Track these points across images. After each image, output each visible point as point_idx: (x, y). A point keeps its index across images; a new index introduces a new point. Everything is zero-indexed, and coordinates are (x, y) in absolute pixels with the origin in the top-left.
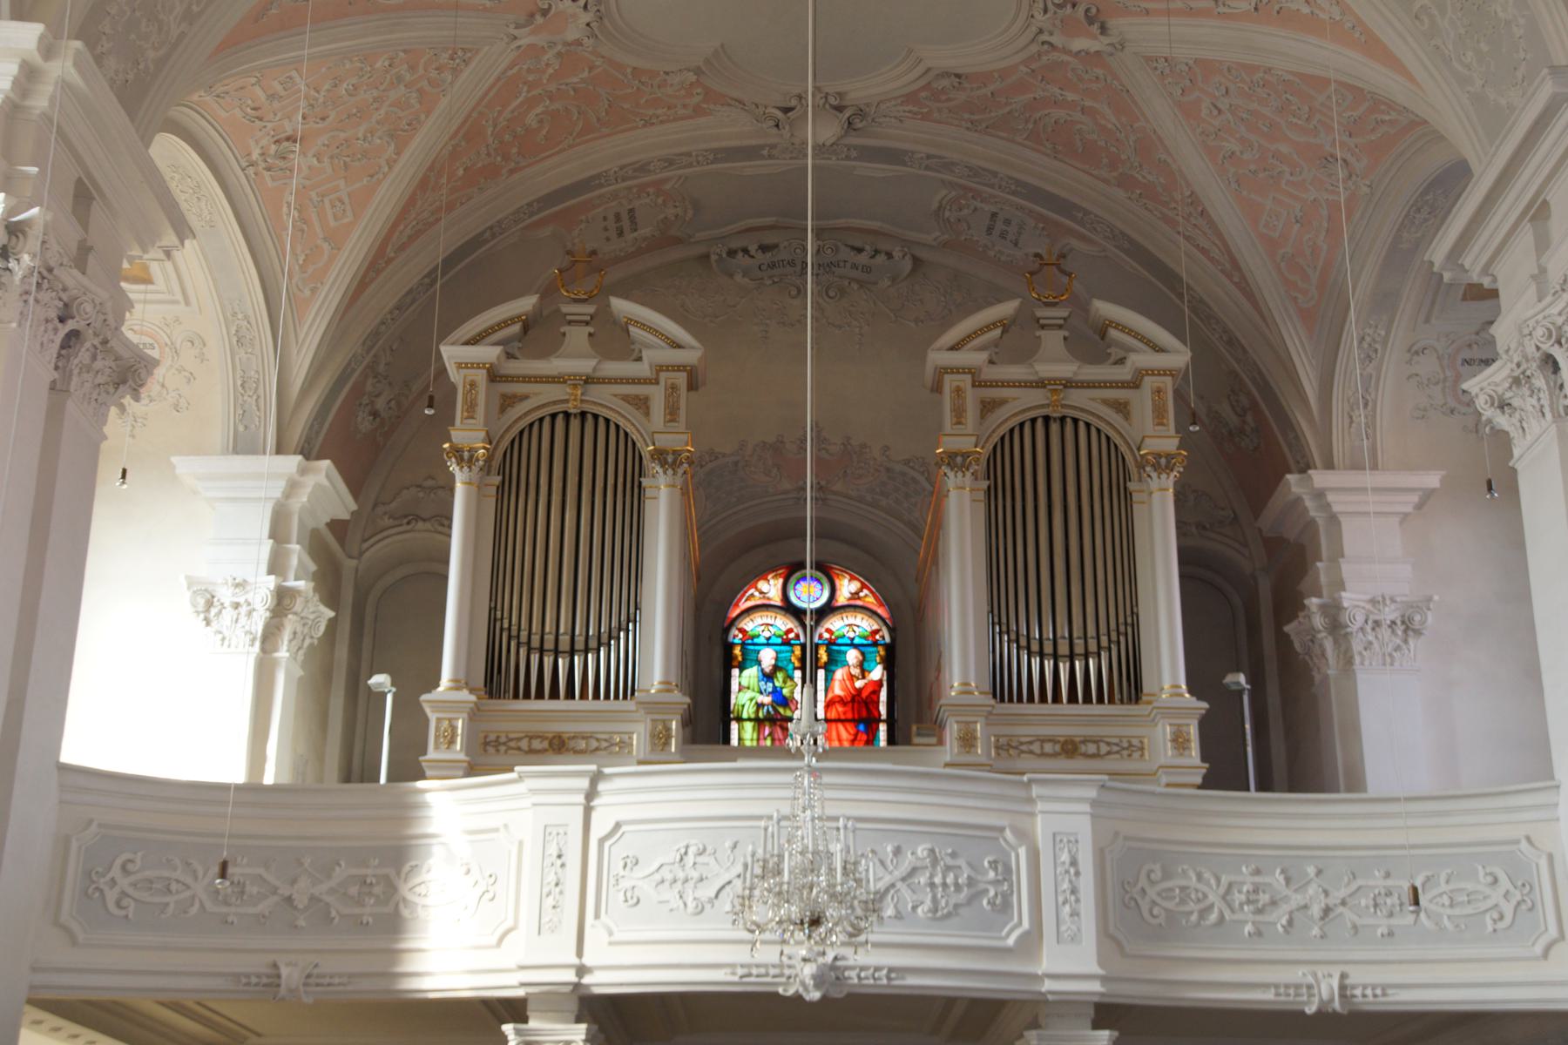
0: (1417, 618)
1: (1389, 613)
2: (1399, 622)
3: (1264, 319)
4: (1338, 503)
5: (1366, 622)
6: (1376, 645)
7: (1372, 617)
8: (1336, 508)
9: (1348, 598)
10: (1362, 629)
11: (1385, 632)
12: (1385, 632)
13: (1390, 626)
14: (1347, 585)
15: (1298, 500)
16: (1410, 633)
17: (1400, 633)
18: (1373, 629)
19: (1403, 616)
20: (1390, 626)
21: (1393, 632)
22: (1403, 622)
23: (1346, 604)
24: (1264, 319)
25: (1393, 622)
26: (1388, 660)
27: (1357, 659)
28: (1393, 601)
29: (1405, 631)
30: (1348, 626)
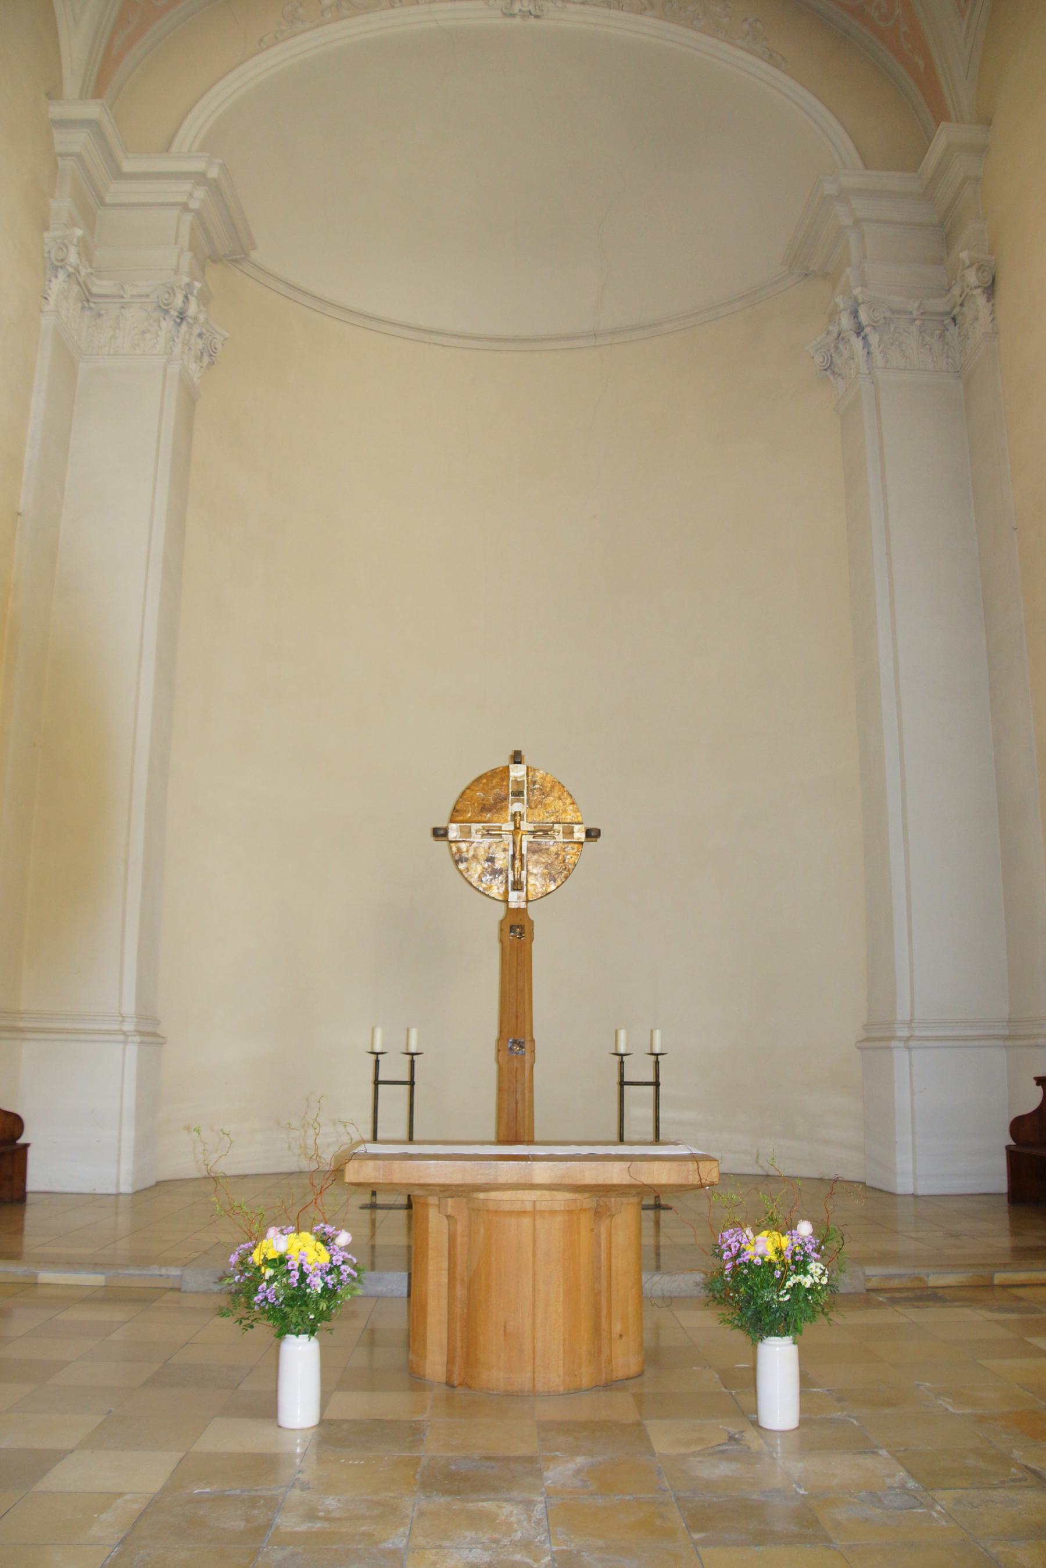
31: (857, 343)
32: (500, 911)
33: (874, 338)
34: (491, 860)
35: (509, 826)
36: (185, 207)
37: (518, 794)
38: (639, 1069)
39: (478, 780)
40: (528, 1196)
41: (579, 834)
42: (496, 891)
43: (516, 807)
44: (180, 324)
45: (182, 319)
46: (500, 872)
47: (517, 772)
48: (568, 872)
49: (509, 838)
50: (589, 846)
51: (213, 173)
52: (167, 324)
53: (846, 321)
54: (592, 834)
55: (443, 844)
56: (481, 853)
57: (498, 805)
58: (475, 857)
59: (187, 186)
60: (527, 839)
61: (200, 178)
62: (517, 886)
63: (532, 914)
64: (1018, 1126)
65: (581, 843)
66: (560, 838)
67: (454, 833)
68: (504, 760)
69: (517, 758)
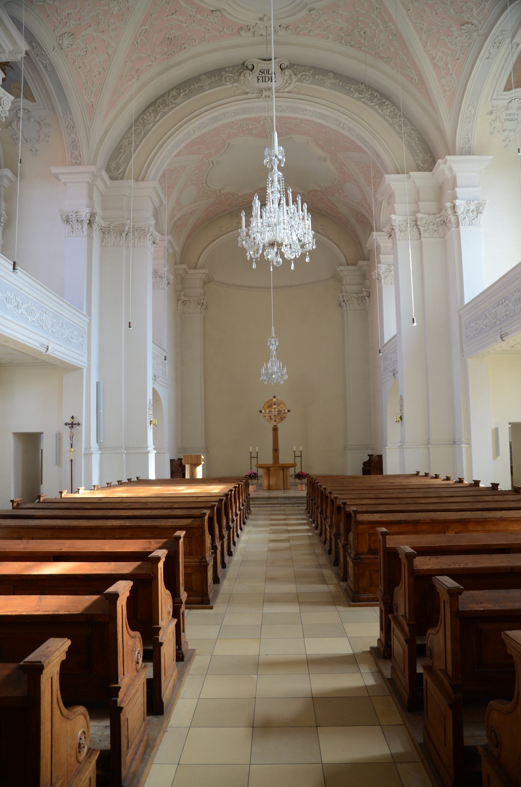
1: (472, 207)
2: (475, 210)
5: (464, 210)
6: (467, 219)
7: (466, 209)
8: (455, 169)
9: (458, 202)
10: (463, 213)
11: (470, 214)
12: (470, 214)
17: (475, 214)
18: (466, 213)
21: (473, 214)
23: (457, 204)
25: (473, 210)
26: (471, 223)
27: (460, 224)
29: (477, 213)
30: (457, 212)
31: (344, 304)
33: (347, 303)
36: (201, 278)
37: (275, 404)
38: (298, 454)
43: (275, 406)
44: (202, 306)
45: (203, 305)
47: (275, 400)
50: (288, 413)
51: (207, 272)
52: (199, 306)
53: (341, 299)
55: (261, 413)
57: (270, 406)
60: (277, 413)
61: (204, 273)
65: (286, 413)
67: (263, 411)
68: (272, 397)
69: (275, 397)
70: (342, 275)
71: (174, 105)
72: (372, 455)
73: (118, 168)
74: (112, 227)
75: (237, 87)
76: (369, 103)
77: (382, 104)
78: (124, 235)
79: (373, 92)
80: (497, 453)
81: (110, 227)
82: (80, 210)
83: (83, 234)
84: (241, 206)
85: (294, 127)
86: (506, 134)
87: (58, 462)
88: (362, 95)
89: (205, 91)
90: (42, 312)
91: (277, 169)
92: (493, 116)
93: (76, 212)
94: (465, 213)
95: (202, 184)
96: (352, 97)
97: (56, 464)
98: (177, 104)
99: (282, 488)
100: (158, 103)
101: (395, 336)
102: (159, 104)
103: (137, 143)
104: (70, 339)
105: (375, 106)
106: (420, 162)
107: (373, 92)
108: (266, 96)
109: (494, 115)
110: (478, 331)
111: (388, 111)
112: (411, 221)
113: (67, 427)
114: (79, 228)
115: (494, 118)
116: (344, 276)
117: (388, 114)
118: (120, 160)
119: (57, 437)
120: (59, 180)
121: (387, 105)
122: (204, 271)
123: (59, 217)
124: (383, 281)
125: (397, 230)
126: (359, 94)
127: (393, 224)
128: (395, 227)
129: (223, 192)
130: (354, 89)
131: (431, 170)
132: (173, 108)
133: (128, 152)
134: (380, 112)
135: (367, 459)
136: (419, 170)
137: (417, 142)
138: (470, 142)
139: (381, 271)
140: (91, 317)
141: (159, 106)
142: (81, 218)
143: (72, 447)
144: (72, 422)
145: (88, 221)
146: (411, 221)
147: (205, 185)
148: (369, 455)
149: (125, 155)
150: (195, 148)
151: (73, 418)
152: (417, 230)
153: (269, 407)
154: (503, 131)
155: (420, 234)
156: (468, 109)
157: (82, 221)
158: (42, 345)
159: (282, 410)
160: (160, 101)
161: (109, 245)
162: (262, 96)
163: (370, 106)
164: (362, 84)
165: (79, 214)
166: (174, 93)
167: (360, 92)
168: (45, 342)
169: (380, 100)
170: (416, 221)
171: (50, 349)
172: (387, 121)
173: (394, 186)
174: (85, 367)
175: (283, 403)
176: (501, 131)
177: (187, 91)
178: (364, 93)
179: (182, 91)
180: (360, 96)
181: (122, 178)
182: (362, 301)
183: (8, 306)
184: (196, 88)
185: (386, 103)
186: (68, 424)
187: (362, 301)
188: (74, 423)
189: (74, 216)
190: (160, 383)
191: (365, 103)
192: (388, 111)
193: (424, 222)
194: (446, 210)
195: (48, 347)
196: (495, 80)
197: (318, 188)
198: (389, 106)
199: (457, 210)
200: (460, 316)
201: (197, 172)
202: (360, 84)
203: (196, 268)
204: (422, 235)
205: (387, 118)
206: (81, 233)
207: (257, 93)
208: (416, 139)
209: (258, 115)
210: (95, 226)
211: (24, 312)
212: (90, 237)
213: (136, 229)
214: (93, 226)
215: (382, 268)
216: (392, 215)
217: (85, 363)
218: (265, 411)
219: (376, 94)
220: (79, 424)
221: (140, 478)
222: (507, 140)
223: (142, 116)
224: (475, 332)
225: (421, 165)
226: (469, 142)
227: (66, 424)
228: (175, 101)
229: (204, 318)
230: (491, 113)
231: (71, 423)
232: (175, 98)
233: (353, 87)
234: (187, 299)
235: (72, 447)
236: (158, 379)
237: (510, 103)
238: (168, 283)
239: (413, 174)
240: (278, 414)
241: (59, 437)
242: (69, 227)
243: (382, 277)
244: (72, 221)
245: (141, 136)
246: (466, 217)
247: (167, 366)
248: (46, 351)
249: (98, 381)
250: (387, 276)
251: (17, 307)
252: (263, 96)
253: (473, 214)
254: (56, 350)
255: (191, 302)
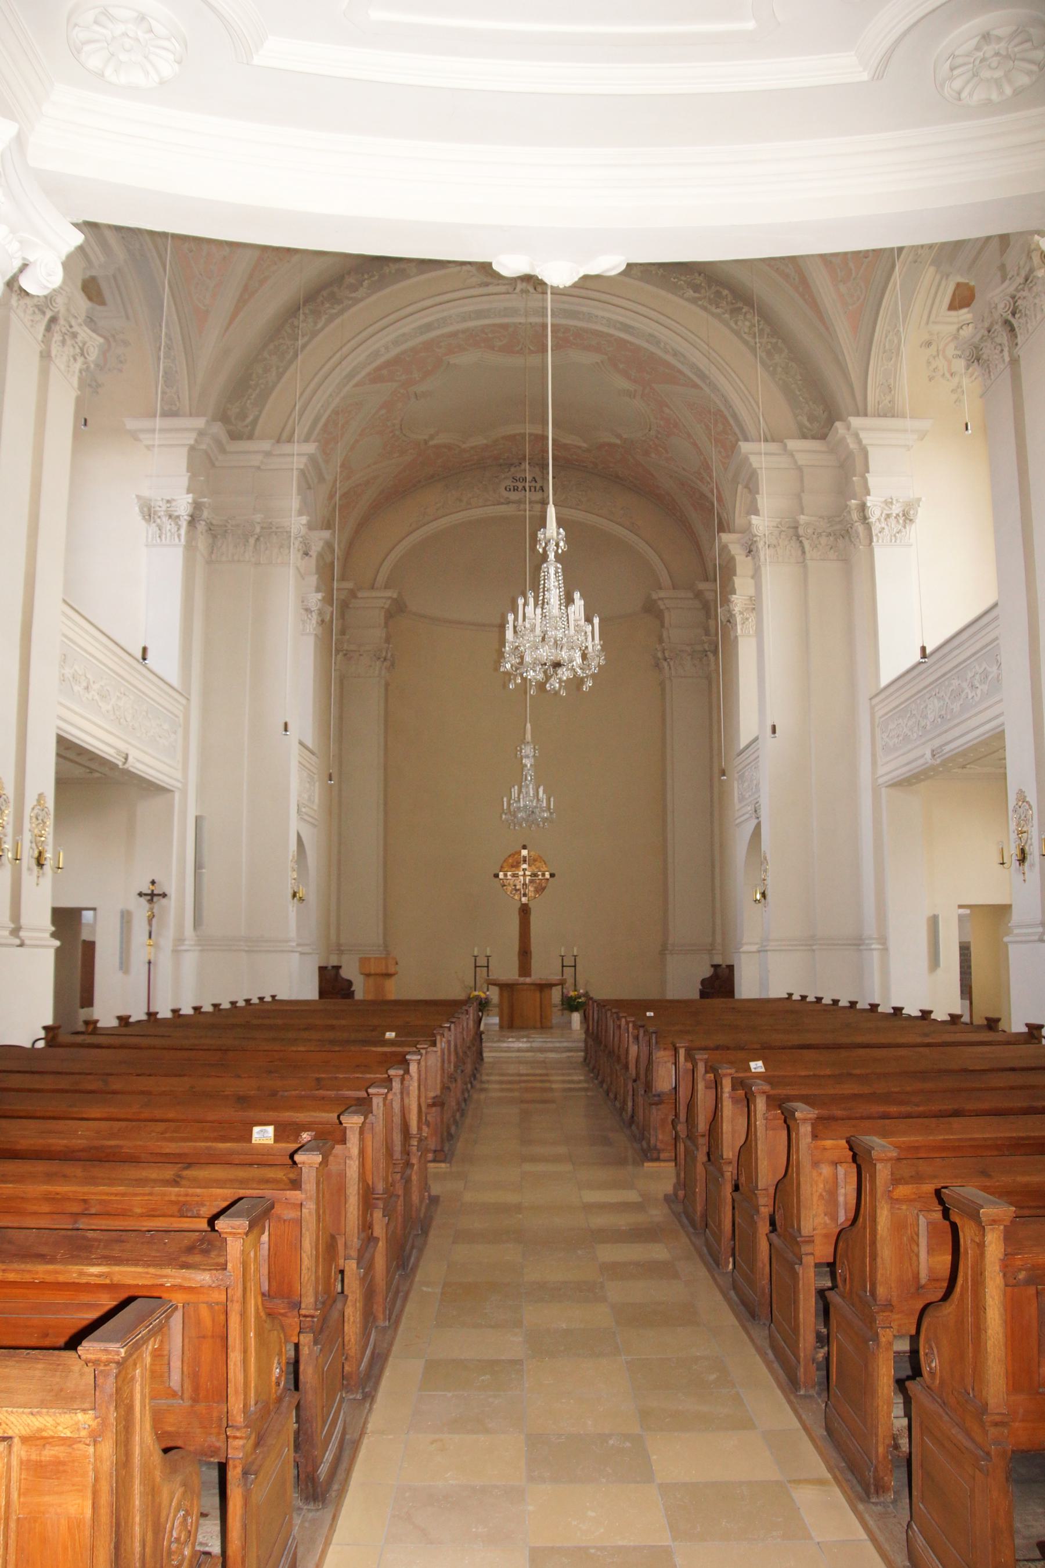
0: (912, 512)
1: (896, 509)
2: (901, 515)
3: (827, 329)
4: (866, 438)
6: (886, 530)
7: (885, 512)
8: (864, 442)
9: (870, 501)
10: (879, 520)
11: (892, 521)
12: (892, 521)
13: (896, 518)
14: (872, 491)
15: (843, 439)
16: (908, 521)
17: (901, 521)
18: (886, 519)
19: (904, 511)
20: (896, 518)
21: (898, 522)
22: (904, 515)
23: (869, 504)
24: (827, 329)
25: (898, 515)
26: (893, 538)
27: (875, 539)
28: (897, 501)
29: (904, 521)
31: (665, 664)
32: (519, 905)
33: (672, 663)
34: (515, 886)
35: (521, 873)
36: (383, 608)
37: (525, 861)
39: (510, 856)
40: (525, 987)
41: (547, 875)
42: (516, 897)
43: (525, 866)
46: (519, 890)
47: (524, 852)
48: (544, 889)
49: (522, 878)
51: (395, 596)
53: (660, 655)
54: (552, 875)
56: (511, 882)
57: (517, 865)
58: (509, 884)
59: (384, 601)
60: (528, 878)
62: (525, 895)
63: (530, 905)
64: (703, 982)
66: (540, 877)
69: (524, 847)
70: (662, 607)
71: (350, 302)
72: (719, 966)
73: (242, 415)
74: (229, 526)
75: (469, 272)
76: (713, 309)
77: (735, 311)
78: (252, 541)
79: (721, 290)
80: (934, 961)
81: (226, 526)
82: (175, 498)
83: (180, 540)
84: (464, 467)
85: (571, 338)
86: (956, 380)
87: (124, 966)
88: (699, 293)
89: (408, 277)
90: (119, 695)
91: (555, 557)
92: (933, 350)
93: (168, 501)
94: (882, 520)
95: (392, 432)
96: (682, 297)
97: (121, 968)
98: (357, 301)
99: (538, 1025)
100: (321, 298)
101: (756, 739)
102: (321, 298)
103: (281, 370)
104: (158, 739)
105: (724, 314)
106: (805, 421)
107: (721, 290)
108: (522, 291)
109: (933, 348)
110: (901, 738)
111: (747, 323)
112: (788, 528)
113: (143, 901)
114: (173, 531)
115: (935, 353)
116: (667, 608)
117: (746, 330)
118: (249, 402)
119: (122, 916)
120: (137, 439)
121: (746, 313)
122: (388, 593)
123: (137, 509)
124: (739, 627)
125: (761, 545)
126: (695, 292)
127: (755, 531)
128: (758, 538)
129: (431, 443)
130: (684, 281)
131: (823, 437)
132: (349, 307)
133: (262, 386)
134: (733, 325)
135: (708, 972)
136: (804, 437)
137: (799, 382)
138: (893, 392)
139: (737, 609)
140: (190, 695)
141: (323, 303)
142: (175, 511)
143: (150, 937)
144: (153, 891)
145: (189, 518)
146: (788, 528)
147: (397, 433)
148: (713, 966)
149: (257, 391)
150: (385, 372)
151: (153, 882)
152: (798, 545)
153: (512, 866)
154: (952, 375)
155: (804, 553)
156: (886, 337)
157: (178, 517)
158: (119, 752)
159: (539, 873)
160: (325, 293)
161: (224, 559)
162: (515, 289)
163: (713, 314)
164: (700, 275)
165: (174, 504)
166: (351, 280)
167: (696, 288)
168: (122, 746)
169: (732, 304)
170: (796, 528)
171: (130, 759)
172: (746, 343)
173: (754, 461)
174: (178, 788)
175: (541, 858)
176: (948, 375)
177: (376, 277)
178: (703, 291)
179: (366, 276)
180: (697, 295)
181: (250, 437)
182: (701, 660)
183: (76, 688)
184: (393, 271)
185: (744, 310)
186: (146, 895)
187: (701, 660)
188: (155, 892)
189: (164, 508)
190: (306, 817)
191: (705, 309)
192: (747, 323)
193: (810, 531)
194: (849, 512)
195: (127, 755)
196: (933, 291)
197: (618, 442)
198: (748, 316)
199: (869, 513)
200: (872, 708)
201: (383, 411)
202: (696, 274)
203: (373, 588)
204: (808, 556)
205: (745, 336)
206: (177, 540)
207: (504, 285)
208: (798, 377)
209: (506, 320)
210: (201, 526)
211: (97, 697)
212: (190, 547)
213: (274, 529)
214: (197, 525)
215: (739, 601)
216: (753, 517)
217: (178, 781)
218: (506, 875)
219: (725, 292)
220: (164, 895)
221: (277, 998)
222: (959, 390)
223: (290, 321)
224: (896, 740)
225: (807, 424)
226: (890, 392)
227: (140, 894)
228: (353, 295)
229: (387, 685)
230: (929, 344)
231: (149, 892)
232: (354, 288)
233: (683, 278)
234: (352, 647)
235: (150, 937)
236: (304, 810)
237: (961, 331)
238: (323, 621)
239: (793, 444)
240: (531, 881)
241: (126, 918)
242: (153, 527)
243: (739, 618)
244: (159, 517)
245: (288, 357)
246: (886, 527)
247: (317, 784)
248: (125, 763)
249: (198, 814)
250: (747, 619)
251: (87, 688)
252: (518, 289)
253: (898, 522)
254: (138, 761)
255: (361, 655)
